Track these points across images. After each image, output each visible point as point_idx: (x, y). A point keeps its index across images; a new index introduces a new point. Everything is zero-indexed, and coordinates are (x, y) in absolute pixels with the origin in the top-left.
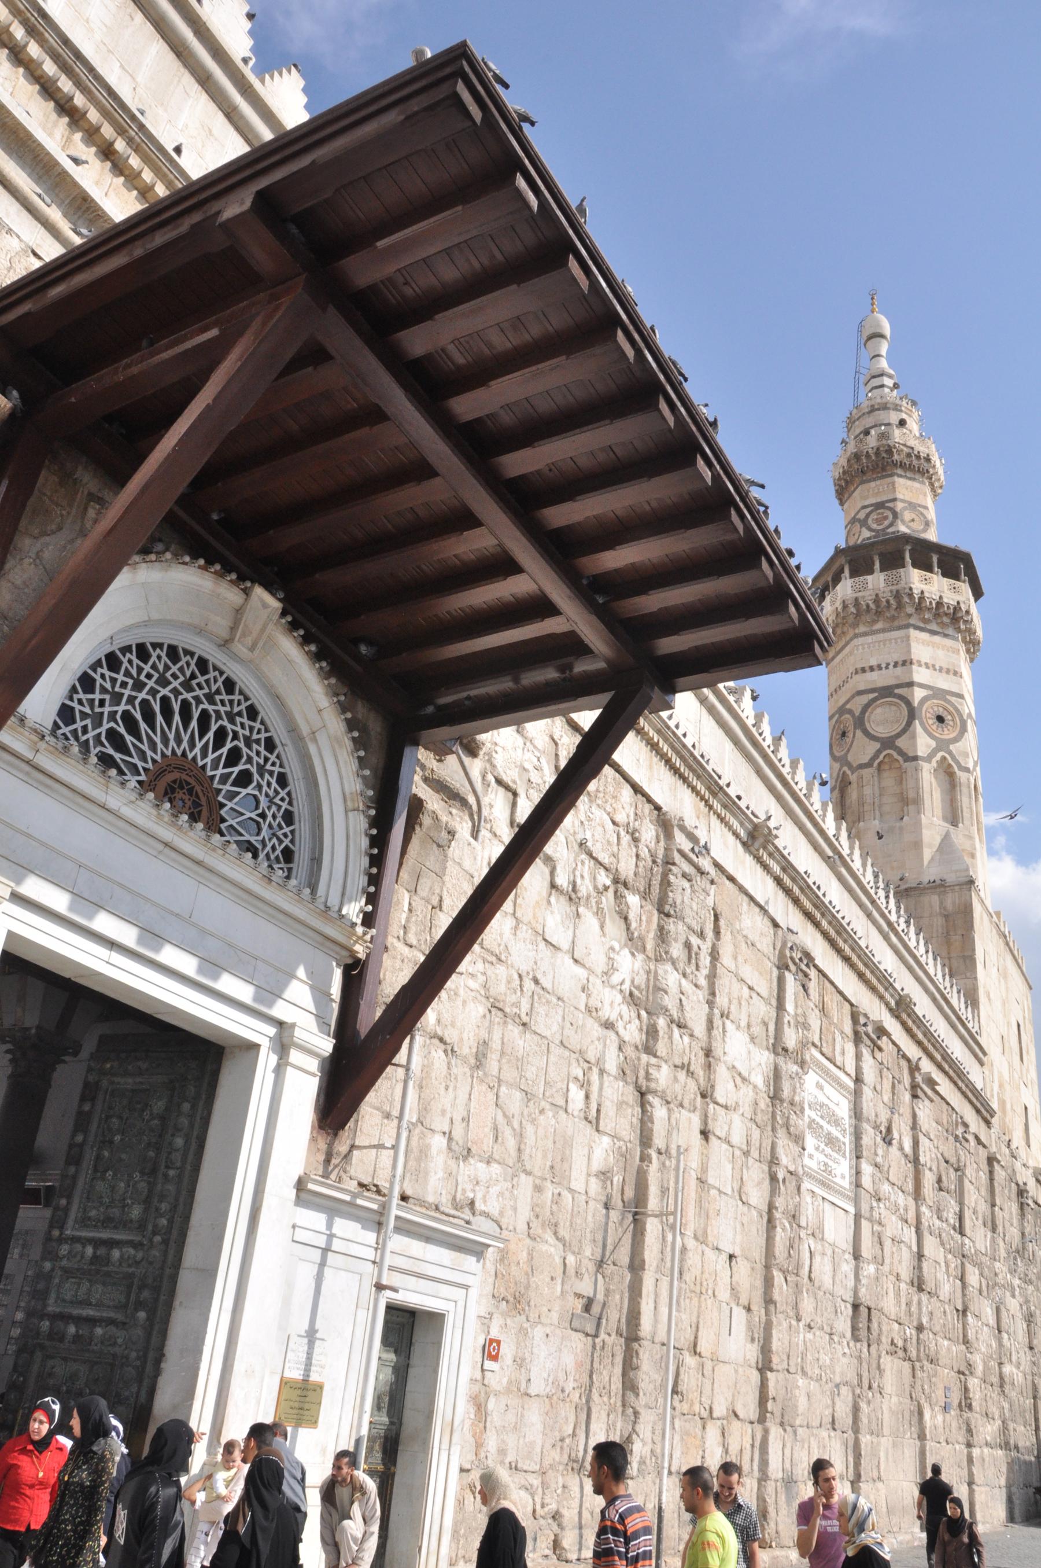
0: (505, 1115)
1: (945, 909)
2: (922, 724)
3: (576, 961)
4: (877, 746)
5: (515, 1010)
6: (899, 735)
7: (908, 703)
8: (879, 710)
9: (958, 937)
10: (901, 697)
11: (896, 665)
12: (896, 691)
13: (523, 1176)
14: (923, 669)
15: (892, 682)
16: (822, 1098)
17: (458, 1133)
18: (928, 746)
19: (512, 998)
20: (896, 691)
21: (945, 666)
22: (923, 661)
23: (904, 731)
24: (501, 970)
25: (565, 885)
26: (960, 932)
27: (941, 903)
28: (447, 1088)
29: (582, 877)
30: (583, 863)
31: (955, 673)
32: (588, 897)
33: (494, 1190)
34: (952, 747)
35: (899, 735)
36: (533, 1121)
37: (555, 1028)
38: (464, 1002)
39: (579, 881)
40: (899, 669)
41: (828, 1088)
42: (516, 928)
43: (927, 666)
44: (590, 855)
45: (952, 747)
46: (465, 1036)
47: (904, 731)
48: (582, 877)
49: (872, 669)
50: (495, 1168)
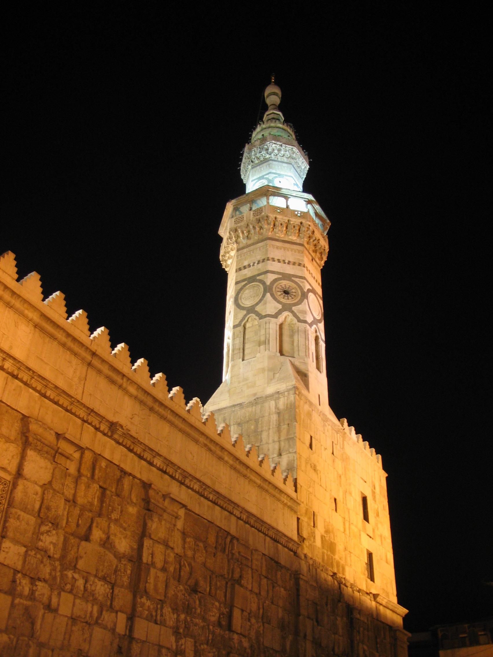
1: (278, 409)
2: (272, 295)
4: (245, 312)
6: (257, 304)
7: (263, 283)
8: (247, 291)
9: (286, 426)
10: (261, 281)
11: (259, 262)
12: (258, 278)
14: (276, 263)
15: (256, 273)
18: (275, 308)
20: (258, 278)
21: (292, 260)
22: (276, 258)
23: (261, 300)
26: (286, 423)
27: (276, 405)
31: (300, 265)
34: (294, 308)
35: (257, 304)
40: (260, 265)
43: (279, 261)
45: (294, 308)
47: (261, 300)
49: (245, 267)
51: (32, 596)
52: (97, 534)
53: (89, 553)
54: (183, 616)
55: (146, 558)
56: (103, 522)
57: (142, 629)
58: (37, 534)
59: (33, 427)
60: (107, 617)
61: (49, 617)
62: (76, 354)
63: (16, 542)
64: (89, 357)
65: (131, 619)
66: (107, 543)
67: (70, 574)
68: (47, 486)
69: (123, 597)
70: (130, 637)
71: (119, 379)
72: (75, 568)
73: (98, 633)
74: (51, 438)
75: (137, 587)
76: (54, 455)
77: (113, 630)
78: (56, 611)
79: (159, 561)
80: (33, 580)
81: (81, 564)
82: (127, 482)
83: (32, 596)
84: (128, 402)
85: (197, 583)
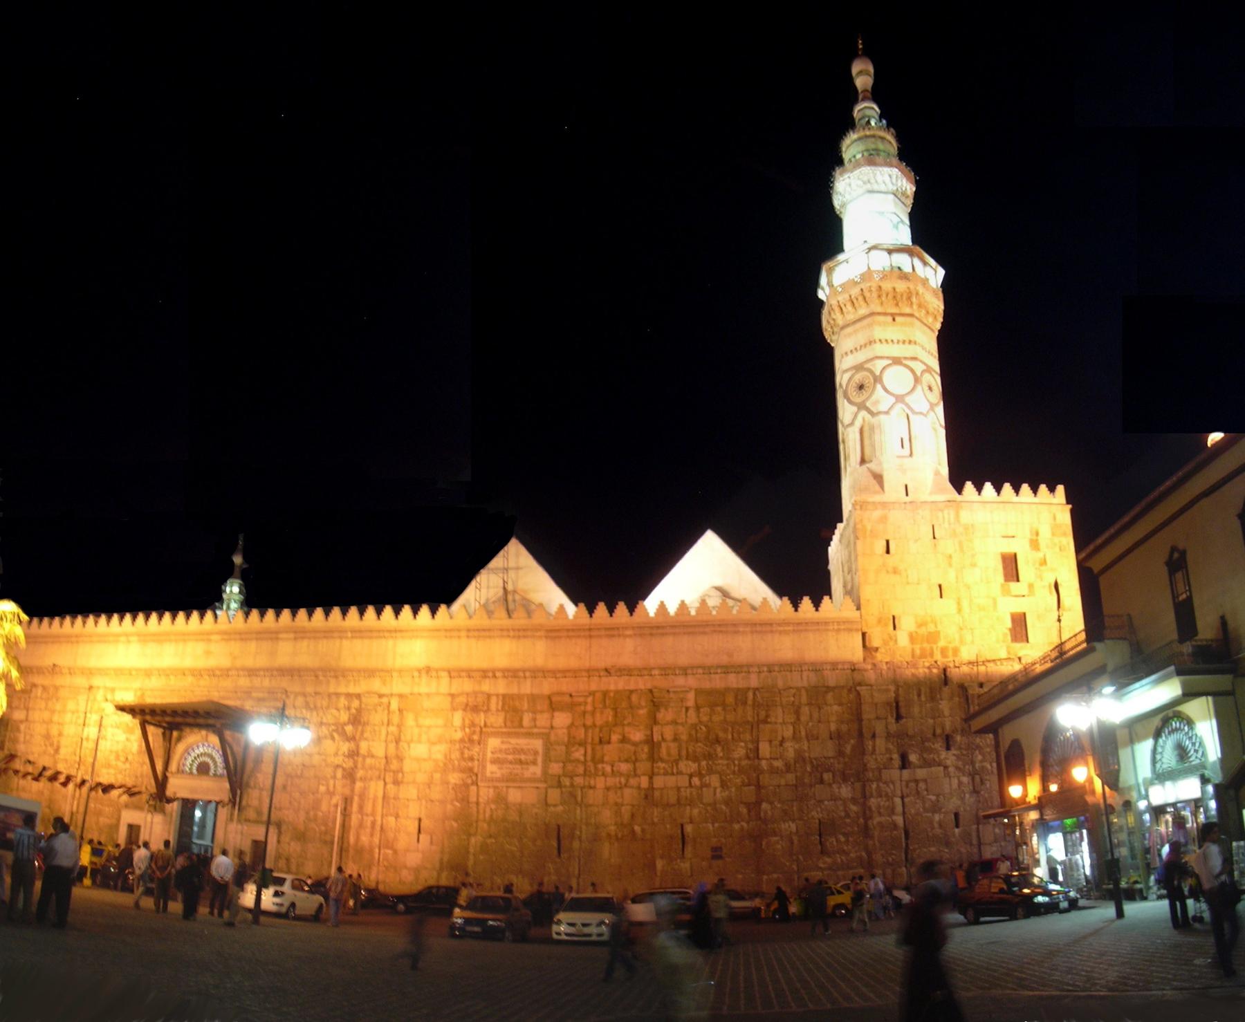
16: (504, 747)
41: (513, 741)
51: (572, 785)
52: (615, 738)
53: (610, 751)
54: (704, 763)
55: (657, 737)
56: (619, 729)
57: (659, 782)
58: (568, 753)
59: (554, 699)
60: (633, 781)
61: (591, 791)
62: (579, 637)
63: (556, 762)
64: (587, 633)
65: (651, 778)
66: (624, 740)
67: (600, 766)
68: (569, 728)
69: (643, 766)
70: (651, 788)
71: (616, 632)
72: (603, 762)
73: (627, 791)
74: (567, 699)
75: (653, 757)
76: (571, 707)
77: (639, 788)
78: (594, 787)
79: (669, 736)
80: (571, 778)
81: (606, 759)
82: (634, 698)
83: (572, 785)
84: (629, 644)
85: (717, 736)
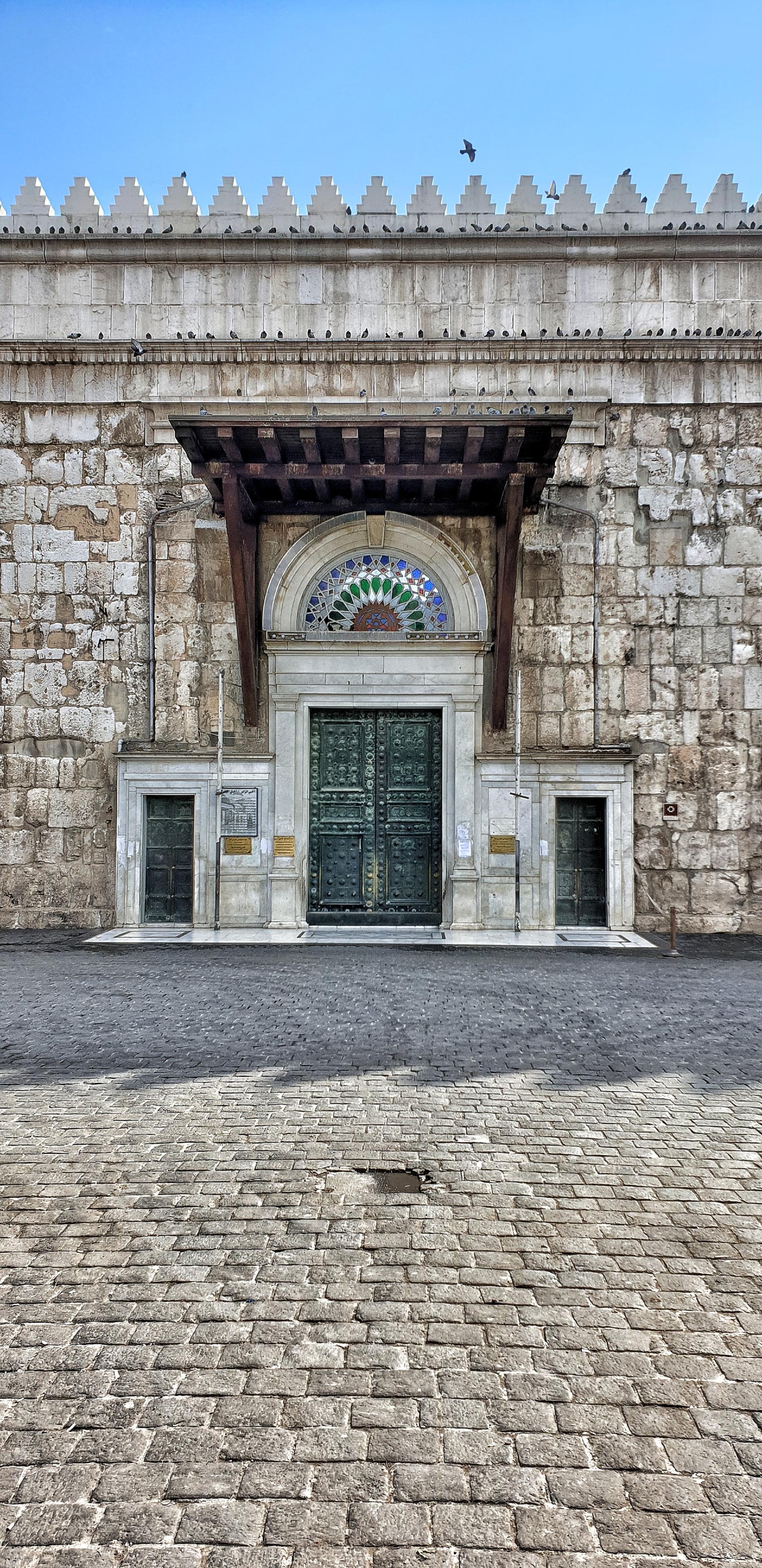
0: (660, 683)
3: (729, 566)
5: (659, 621)
13: (687, 714)
17: (616, 704)
19: (657, 614)
24: (642, 603)
25: (706, 521)
28: (588, 686)
29: (726, 506)
30: (725, 496)
32: (737, 517)
33: (657, 728)
36: (692, 679)
37: (709, 616)
38: (606, 634)
39: (721, 510)
42: (652, 572)
44: (736, 486)
46: (611, 652)
48: (726, 506)
50: (656, 716)
